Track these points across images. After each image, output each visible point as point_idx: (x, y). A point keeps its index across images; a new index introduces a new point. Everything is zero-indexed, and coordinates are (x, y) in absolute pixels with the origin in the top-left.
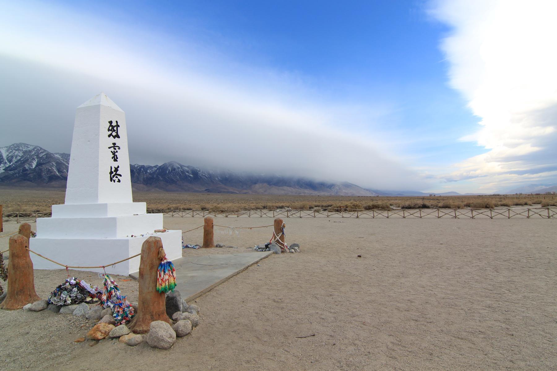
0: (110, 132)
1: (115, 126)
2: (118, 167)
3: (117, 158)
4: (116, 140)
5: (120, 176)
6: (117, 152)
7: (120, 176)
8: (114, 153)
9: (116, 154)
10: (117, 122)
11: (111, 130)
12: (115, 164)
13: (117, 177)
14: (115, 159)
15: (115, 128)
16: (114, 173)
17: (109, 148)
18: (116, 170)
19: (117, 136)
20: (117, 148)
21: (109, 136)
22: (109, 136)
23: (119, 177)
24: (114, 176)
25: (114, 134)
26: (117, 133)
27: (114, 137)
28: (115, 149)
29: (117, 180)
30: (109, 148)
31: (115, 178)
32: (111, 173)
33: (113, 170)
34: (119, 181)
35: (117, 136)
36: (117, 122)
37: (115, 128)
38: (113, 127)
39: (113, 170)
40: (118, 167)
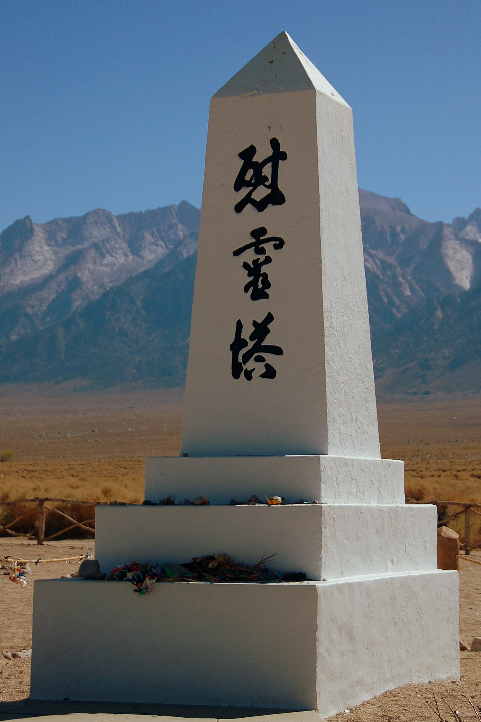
0: (245, 191)
1: (265, 162)
2: (270, 318)
3: (267, 284)
4: (272, 219)
5: (277, 351)
6: (268, 260)
7: (277, 351)
8: (254, 270)
9: (264, 269)
10: (275, 143)
11: (248, 184)
12: (258, 310)
13: (260, 359)
14: (258, 286)
15: (267, 171)
16: (251, 344)
17: (237, 253)
18: (261, 329)
19: (276, 198)
20: (269, 247)
21: (239, 208)
22: (239, 208)
23: (270, 358)
24: (246, 358)
25: (261, 193)
26: (274, 186)
27: (261, 206)
28: (262, 251)
29: (260, 368)
30: (237, 253)
31: (251, 365)
32: (238, 344)
33: (246, 334)
34: (270, 373)
35: (276, 198)
36: (275, 143)
37: (267, 171)
38: (258, 167)
39: (247, 333)
40: (270, 318)
